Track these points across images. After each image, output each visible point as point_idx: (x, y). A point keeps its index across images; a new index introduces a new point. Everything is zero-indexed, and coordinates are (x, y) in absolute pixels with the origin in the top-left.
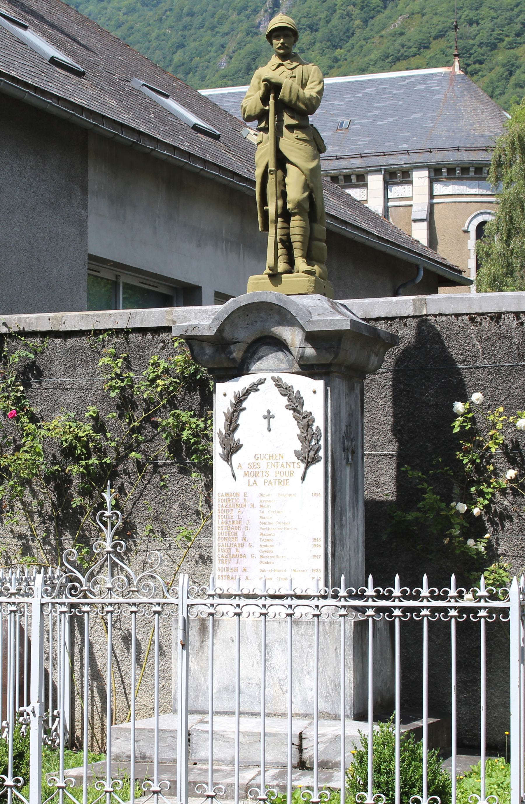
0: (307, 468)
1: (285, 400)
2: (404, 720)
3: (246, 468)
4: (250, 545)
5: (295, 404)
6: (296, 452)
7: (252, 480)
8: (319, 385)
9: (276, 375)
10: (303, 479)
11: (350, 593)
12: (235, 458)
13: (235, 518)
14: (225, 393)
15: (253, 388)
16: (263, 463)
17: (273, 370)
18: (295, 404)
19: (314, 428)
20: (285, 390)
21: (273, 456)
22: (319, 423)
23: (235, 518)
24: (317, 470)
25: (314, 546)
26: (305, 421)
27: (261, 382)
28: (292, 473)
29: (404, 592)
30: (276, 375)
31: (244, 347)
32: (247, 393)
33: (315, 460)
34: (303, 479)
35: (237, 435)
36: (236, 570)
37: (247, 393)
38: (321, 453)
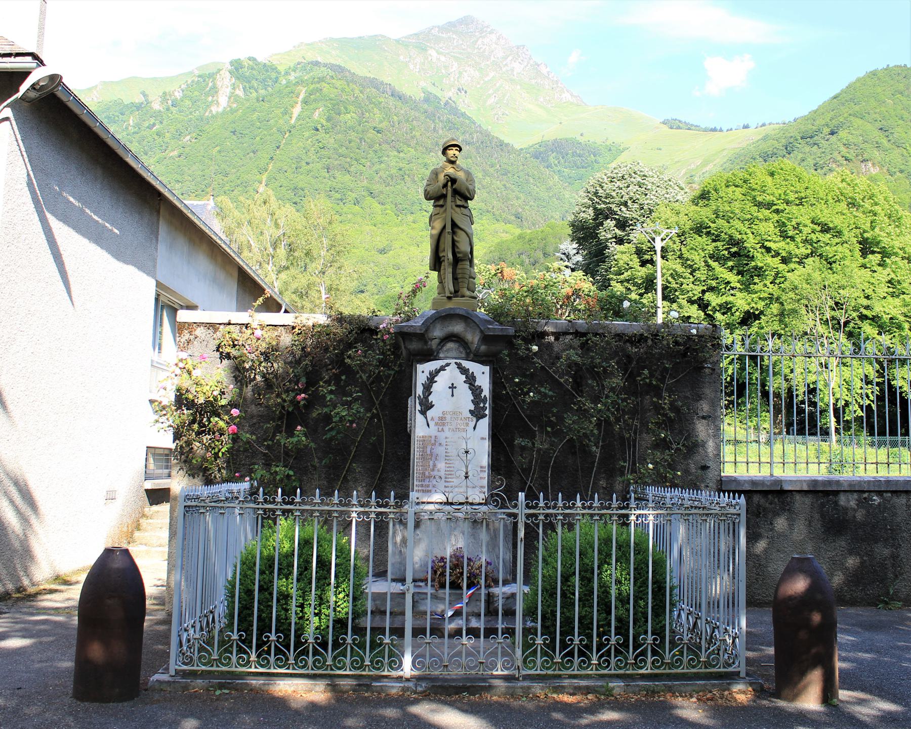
0: (477, 421)
1: (463, 378)
2: (526, 583)
3: (436, 420)
4: (439, 471)
5: (471, 380)
6: (470, 411)
7: (440, 428)
8: (487, 369)
9: (458, 361)
10: (474, 428)
11: (265, 500)
12: (430, 413)
13: (429, 452)
14: (423, 371)
15: (442, 368)
16: (448, 417)
17: (456, 358)
18: (471, 380)
19: (483, 395)
20: (464, 371)
21: (454, 413)
22: (486, 392)
23: (429, 452)
24: (484, 425)
25: (482, 471)
26: (476, 391)
27: (448, 365)
28: (467, 425)
29: (341, 501)
30: (458, 361)
31: (437, 341)
32: (437, 372)
33: (484, 416)
34: (474, 428)
35: (431, 398)
36: (428, 486)
37: (437, 372)
38: (487, 412)
